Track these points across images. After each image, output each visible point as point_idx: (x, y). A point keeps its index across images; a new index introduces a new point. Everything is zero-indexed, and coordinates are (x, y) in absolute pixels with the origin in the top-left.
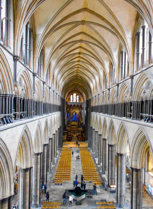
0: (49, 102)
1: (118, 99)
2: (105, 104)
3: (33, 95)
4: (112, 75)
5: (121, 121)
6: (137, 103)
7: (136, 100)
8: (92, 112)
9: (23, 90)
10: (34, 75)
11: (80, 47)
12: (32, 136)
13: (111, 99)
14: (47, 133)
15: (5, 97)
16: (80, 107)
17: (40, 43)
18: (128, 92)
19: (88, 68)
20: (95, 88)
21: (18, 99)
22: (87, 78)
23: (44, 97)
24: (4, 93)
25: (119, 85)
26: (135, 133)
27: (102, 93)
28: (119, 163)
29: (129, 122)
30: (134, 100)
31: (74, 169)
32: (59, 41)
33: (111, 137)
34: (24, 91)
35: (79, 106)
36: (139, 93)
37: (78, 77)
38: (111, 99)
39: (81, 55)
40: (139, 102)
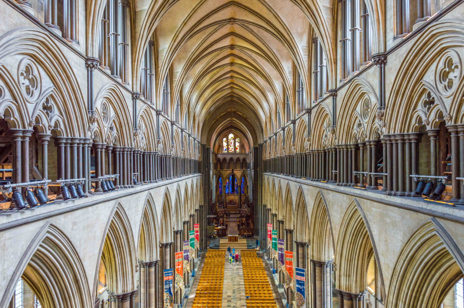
1: (312, 142)
2: (287, 154)
6: (347, 148)
9: (111, 128)
10: (135, 97)
11: (232, 34)
13: (298, 143)
15: (71, 144)
16: (243, 163)
17: (145, 29)
18: (329, 125)
21: (102, 149)
23: (158, 142)
24: (69, 136)
30: (340, 143)
34: (115, 131)
35: (241, 161)
37: (235, 99)
38: (298, 143)
39: (236, 52)
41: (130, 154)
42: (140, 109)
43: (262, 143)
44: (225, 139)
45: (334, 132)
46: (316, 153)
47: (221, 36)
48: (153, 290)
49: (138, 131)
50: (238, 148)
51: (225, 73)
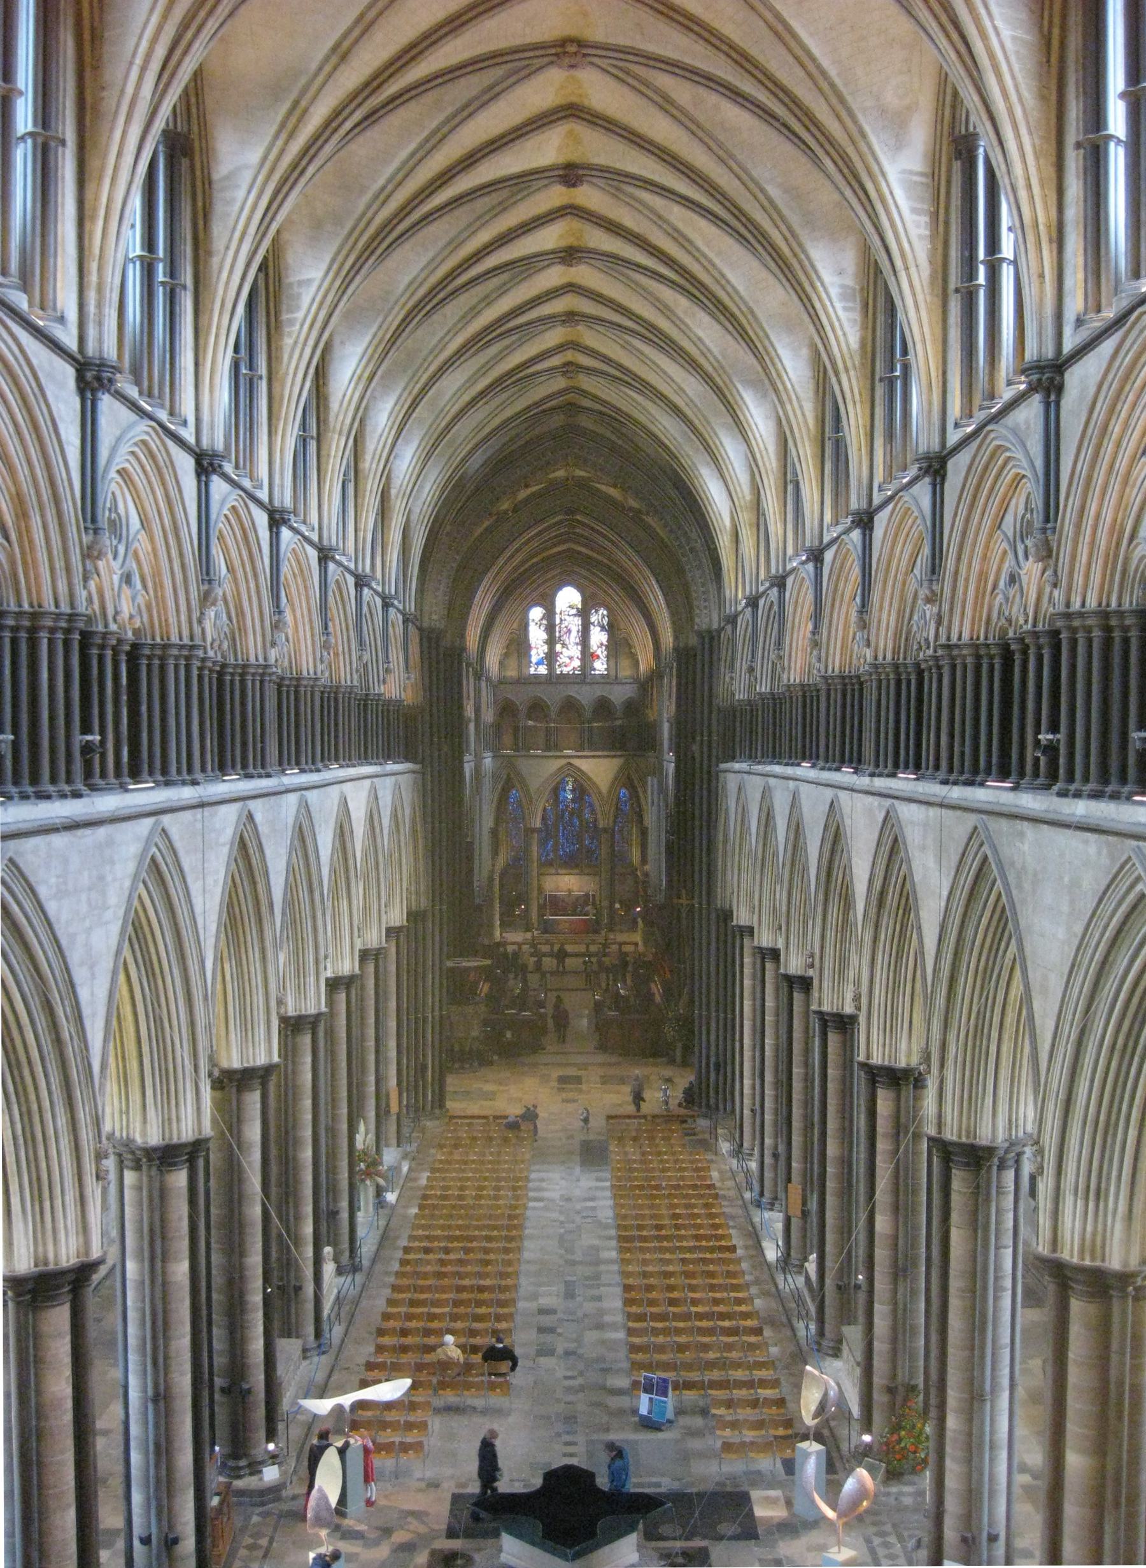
0: (273, 654)
1: (946, 607)
3: (77, 580)
4: (891, 382)
5: (972, 819)
6: (1108, 629)
7: (1092, 603)
8: (733, 758)
12: (80, 975)
13: (885, 617)
14: (264, 959)
19: (663, 324)
20: (746, 518)
22: (667, 427)
23: (206, 599)
25: (950, 464)
26: (1079, 929)
27: (810, 567)
28: (956, 1235)
29: (1035, 820)
30: (1076, 605)
31: (542, 1311)
32: (341, 53)
33: (894, 987)
36: (1116, 530)
37: (585, 422)
38: (885, 617)
39: (589, 196)
40: (1121, 614)
41: (67, 643)
42: (119, 440)
43: (715, 626)
44: (536, 613)
45: (1049, 556)
46: (965, 656)
47: (517, 119)
48: (181, 1269)
49: (106, 540)
50: (602, 653)
51: (539, 297)
